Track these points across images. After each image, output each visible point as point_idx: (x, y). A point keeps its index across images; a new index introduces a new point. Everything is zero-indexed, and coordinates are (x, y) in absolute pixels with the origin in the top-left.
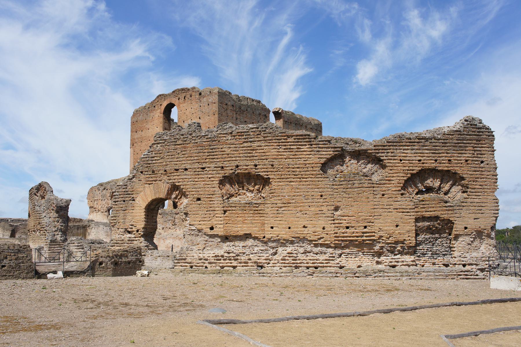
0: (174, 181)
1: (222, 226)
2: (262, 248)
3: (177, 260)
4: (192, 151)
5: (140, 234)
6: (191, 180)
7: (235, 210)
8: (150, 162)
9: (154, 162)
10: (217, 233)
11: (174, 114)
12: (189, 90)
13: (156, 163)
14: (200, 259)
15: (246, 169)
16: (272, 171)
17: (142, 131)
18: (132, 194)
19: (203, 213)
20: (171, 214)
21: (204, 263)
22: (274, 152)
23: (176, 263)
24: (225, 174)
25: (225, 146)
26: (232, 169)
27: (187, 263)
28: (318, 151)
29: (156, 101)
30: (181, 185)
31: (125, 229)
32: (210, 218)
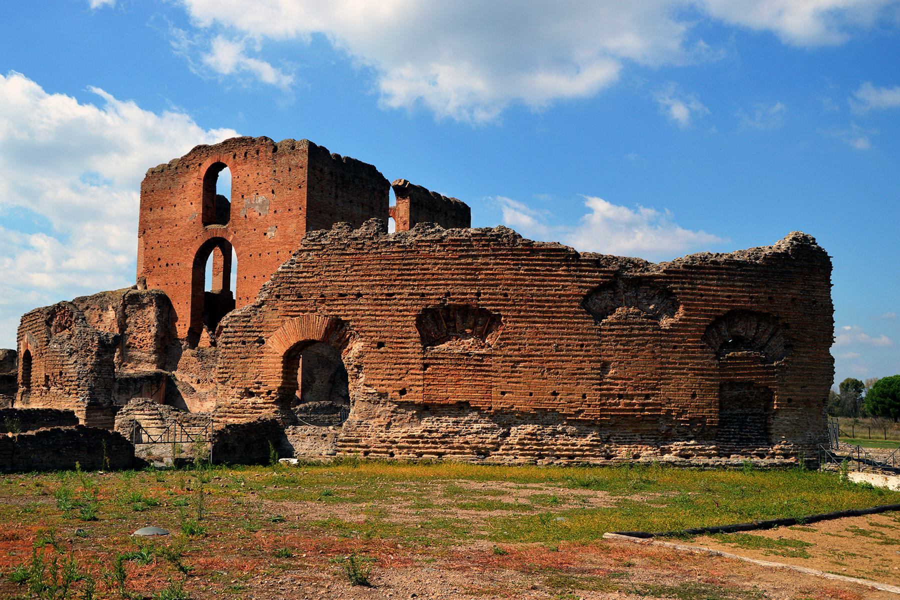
0: (336, 313)
1: (421, 389)
2: (486, 426)
3: (341, 441)
4: (370, 267)
5: (273, 398)
6: (367, 313)
7: (442, 364)
8: (295, 280)
9: (302, 280)
10: (412, 400)
11: (225, 184)
12: (253, 141)
13: (305, 282)
14: (384, 441)
15: (463, 300)
16: (505, 305)
17: (162, 208)
18: (260, 332)
19: (389, 366)
20: (214, 356)
21: (390, 448)
22: (508, 275)
23: (340, 447)
24: (427, 305)
25: (428, 261)
26: (439, 299)
27: (360, 447)
28: (577, 276)
29: (191, 157)
30: (351, 320)
31: (246, 389)
32: (401, 376)
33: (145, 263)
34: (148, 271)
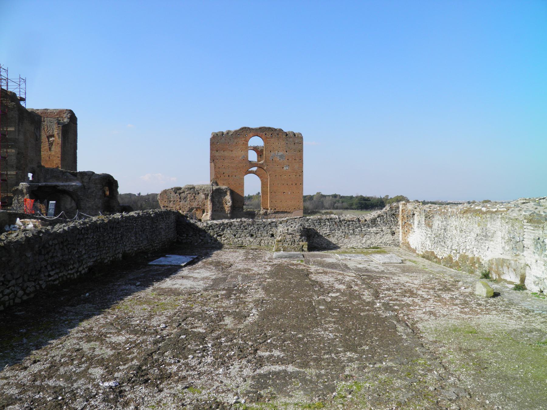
12: (276, 130)
33: (215, 174)
34: (217, 178)
